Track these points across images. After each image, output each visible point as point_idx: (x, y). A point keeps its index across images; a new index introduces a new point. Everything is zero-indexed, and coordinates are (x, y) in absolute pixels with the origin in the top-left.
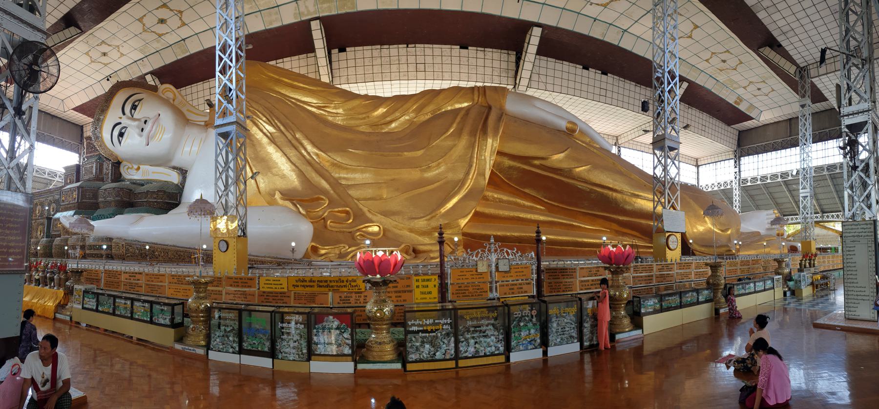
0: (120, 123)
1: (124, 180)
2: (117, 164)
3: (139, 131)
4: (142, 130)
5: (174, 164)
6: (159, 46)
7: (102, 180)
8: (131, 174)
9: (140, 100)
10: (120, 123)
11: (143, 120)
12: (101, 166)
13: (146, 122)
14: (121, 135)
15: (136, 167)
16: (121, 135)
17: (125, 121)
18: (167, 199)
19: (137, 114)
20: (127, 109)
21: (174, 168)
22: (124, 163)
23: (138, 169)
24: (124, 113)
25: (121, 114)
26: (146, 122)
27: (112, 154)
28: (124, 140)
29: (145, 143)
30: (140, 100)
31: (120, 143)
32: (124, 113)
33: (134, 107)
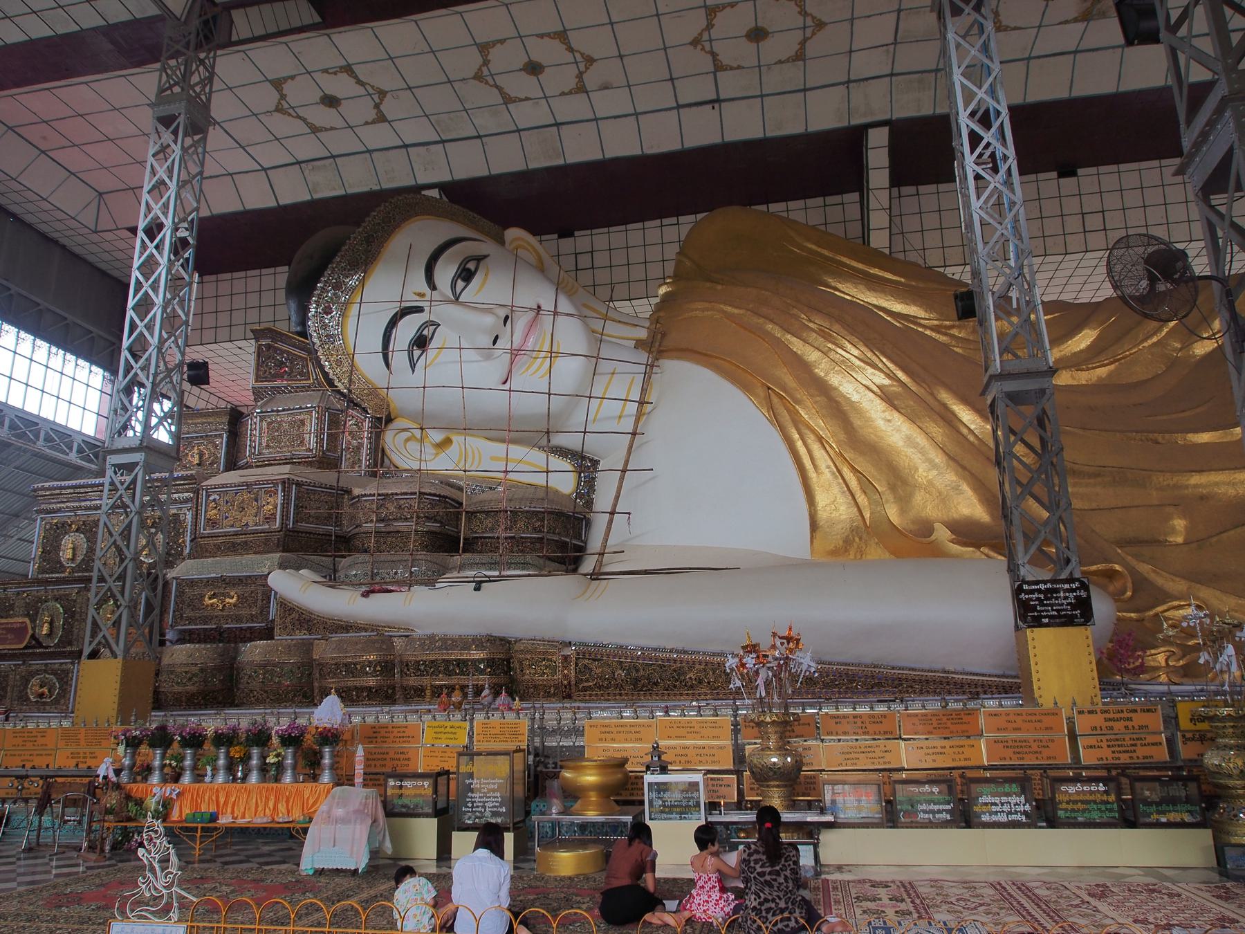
3: (487, 341)
6: (486, 123)
9: (479, 259)
10: (419, 310)
11: (502, 313)
12: (335, 422)
14: (421, 342)
15: (437, 436)
16: (421, 342)
18: (559, 538)
19: (470, 293)
20: (445, 273)
22: (399, 423)
23: (447, 442)
25: (425, 288)
27: (373, 392)
30: (479, 259)
31: (413, 366)
33: (466, 275)
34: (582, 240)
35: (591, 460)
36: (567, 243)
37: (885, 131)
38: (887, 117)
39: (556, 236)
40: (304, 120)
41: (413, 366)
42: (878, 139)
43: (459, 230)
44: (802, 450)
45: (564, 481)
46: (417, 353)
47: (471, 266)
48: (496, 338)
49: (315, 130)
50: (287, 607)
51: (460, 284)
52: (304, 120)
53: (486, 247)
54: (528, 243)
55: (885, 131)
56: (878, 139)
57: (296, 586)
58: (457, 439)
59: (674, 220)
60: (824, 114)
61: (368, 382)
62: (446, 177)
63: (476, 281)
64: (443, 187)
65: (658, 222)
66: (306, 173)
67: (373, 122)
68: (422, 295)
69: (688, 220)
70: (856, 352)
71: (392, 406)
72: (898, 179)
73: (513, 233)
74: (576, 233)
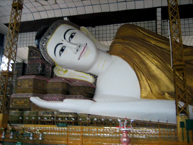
0: (62, 44)
1: (56, 77)
2: (54, 66)
3: (75, 50)
4: (77, 50)
5: (91, 71)
7: (44, 75)
8: (60, 73)
10: (62, 44)
11: (79, 45)
13: (80, 46)
14: (62, 50)
16: (62, 50)
17: (65, 43)
19: (73, 40)
20: (68, 36)
21: (91, 74)
22: (57, 66)
24: (65, 39)
26: (80, 46)
28: (63, 54)
29: (78, 57)
30: (74, 33)
31: (60, 55)
32: (65, 39)
33: (72, 37)
34: (97, 28)
35: (96, 76)
36: (94, 29)
37: (161, 8)
38: (161, 6)
39: (91, 27)
40: (41, 3)
41: (60, 55)
42: (159, 10)
43: (71, 27)
44: (139, 76)
45: (90, 80)
46: (61, 52)
47: (73, 35)
48: (77, 50)
49: (42, 5)
50: (34, 105)
51: (71, 38)
52: (41, 3)
53: (76, 31)
54: (86, 30)
55: (161, 8)
56: (159, 10)
57: (36, 100)
58: (68, 70)
59: (116, 25)
60: (148, 5)
61: (51, 58)
62: (69, 15)
63: (74, 38)
64: (68, 17)
65: (113, 25)
66: (40, 13)
67: (55, 4)
68: (63, 41)
69: (119, 25)
70: (151, 56)
71: (56, 63)
72: (162, 19)
73: (82, 27)
74: (96, 27)
